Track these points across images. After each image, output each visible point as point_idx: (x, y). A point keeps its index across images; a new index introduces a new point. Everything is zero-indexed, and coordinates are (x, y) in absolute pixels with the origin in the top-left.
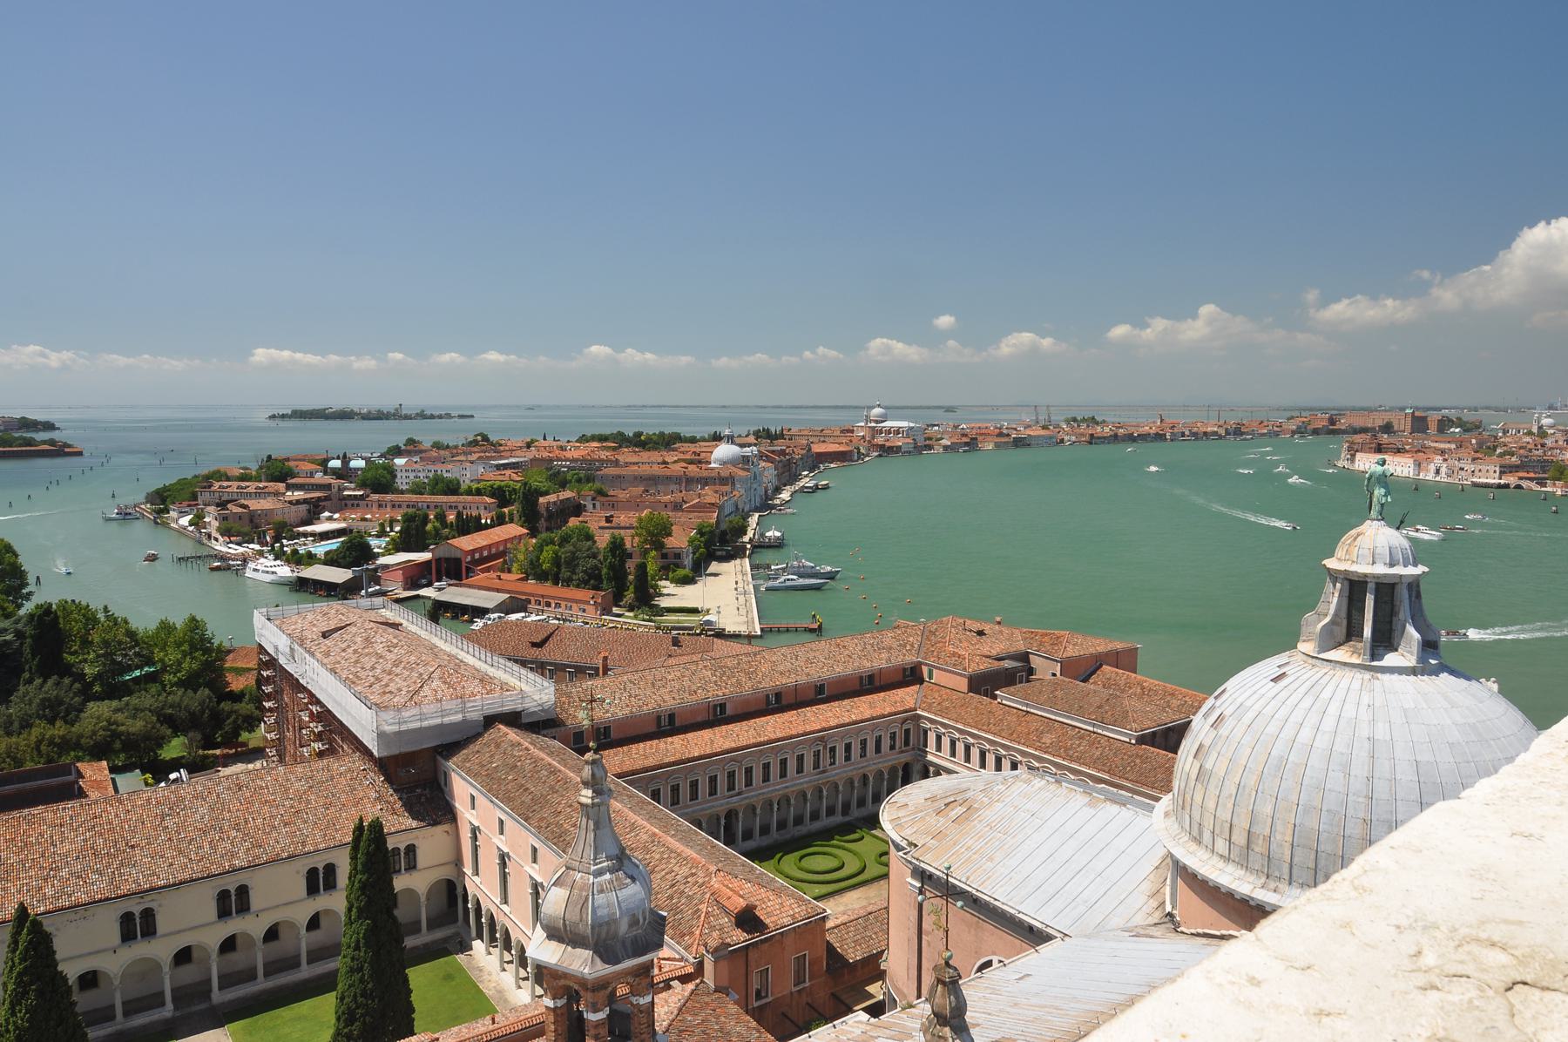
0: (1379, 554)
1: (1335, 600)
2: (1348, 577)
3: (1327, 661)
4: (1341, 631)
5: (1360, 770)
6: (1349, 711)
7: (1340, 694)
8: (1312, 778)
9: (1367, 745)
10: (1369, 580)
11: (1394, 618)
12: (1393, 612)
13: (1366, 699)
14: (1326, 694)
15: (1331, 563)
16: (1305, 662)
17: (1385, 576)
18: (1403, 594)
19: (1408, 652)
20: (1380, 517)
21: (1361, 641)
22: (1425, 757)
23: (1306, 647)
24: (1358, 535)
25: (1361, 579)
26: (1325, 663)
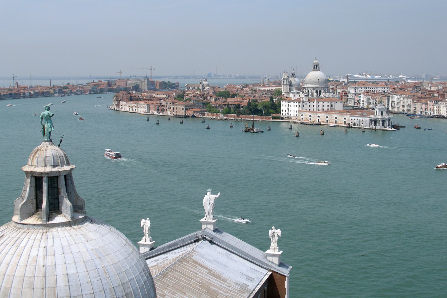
0: (48, 161)
1: (28, 189)
2: (34, 175)
3: (25, 224)
4: (32, 207)
5: (38, 284)
6: (34, 253)
7: (31, 242)
8: (14, 294)
9: (43, 270)
10: (44, 176)
11: (59, 195)
12: (58, 193)
13: (43, 244)
14: (23, 244)
15: (27, 168)
16: (16, 227)
17: (51, 172)
18: (62, 181)
19: (67, 214)
20: (49, 140)
21: (41, 211)
22: (72, 271)
23: (16, 218)
24: (38, 150)
25: (40, 176)
26: (24, 226)
